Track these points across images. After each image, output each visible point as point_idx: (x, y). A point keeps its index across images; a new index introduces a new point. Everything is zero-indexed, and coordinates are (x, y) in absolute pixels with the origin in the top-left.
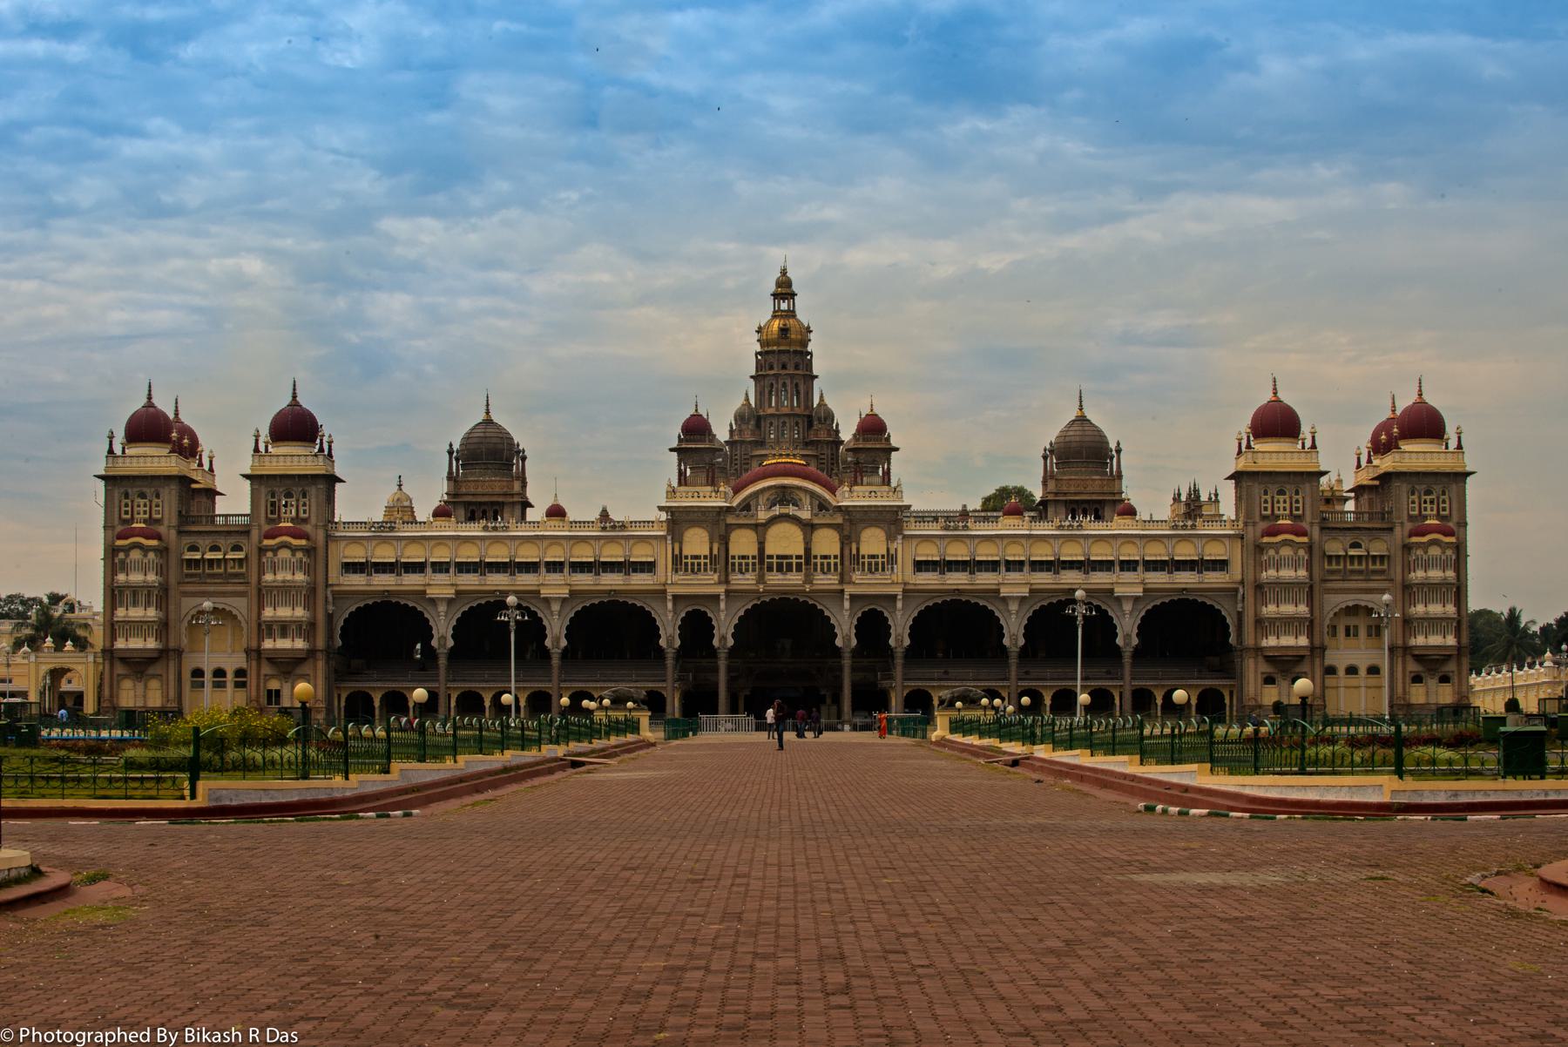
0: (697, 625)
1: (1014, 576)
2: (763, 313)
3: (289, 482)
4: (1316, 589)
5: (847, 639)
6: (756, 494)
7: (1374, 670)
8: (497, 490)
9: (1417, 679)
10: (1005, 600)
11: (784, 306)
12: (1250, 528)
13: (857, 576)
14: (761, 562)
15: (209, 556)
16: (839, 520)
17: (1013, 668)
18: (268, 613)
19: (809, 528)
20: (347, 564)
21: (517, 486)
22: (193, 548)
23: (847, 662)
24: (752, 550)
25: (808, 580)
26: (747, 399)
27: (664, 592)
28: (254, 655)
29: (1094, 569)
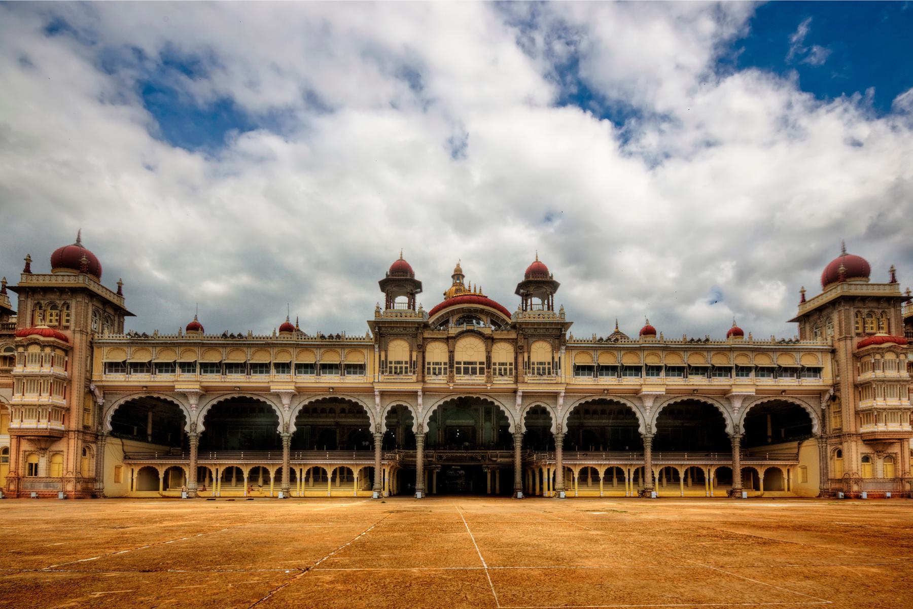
1: (653, 379)
13: (528, 378)
14: (451, 366)
19: (490, 340)
25: (489, 380)
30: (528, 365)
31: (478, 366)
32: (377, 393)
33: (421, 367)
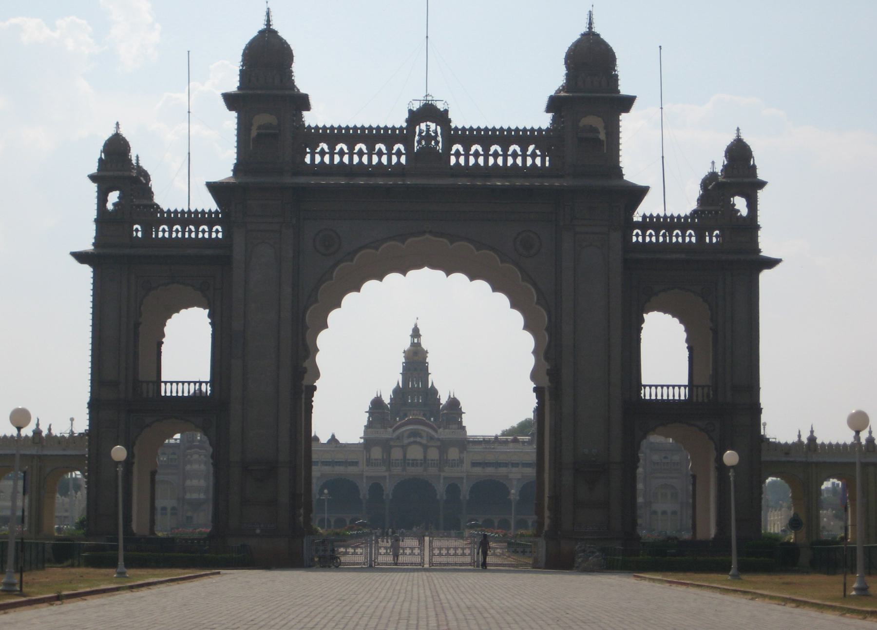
0: (376, 488)
1: (515, 470)
2: (406, 343)
7: (674, 513)
11: (416, 340)
16: (439, 444)
18: (188, 483)
19: (426, 447)
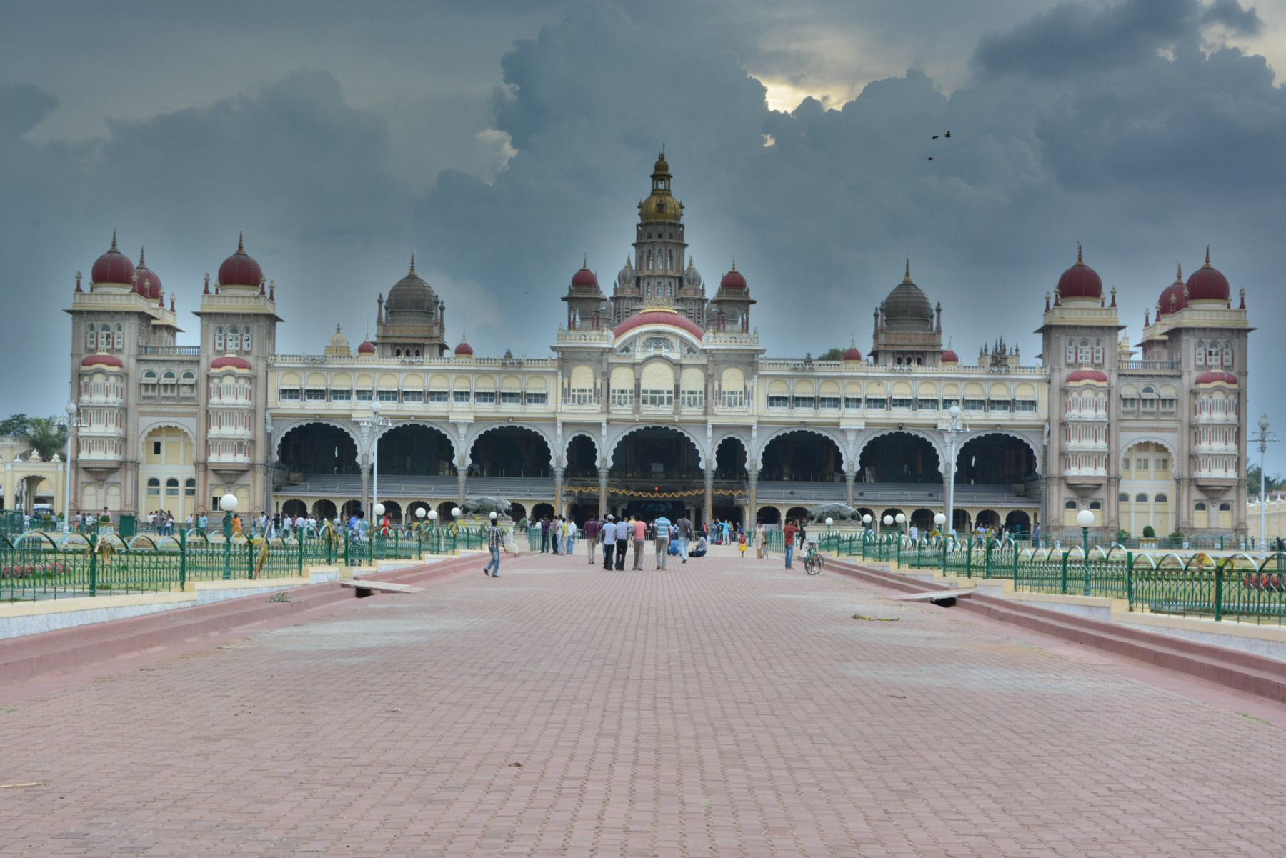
0: (582, 450)
1: (852, 411)
3: (234, 320)
4: (1113, 427)
5: (709, 462)
6: (634, 338)
7: (1161, 498)
8: (419, 334)
9: (1201, 506)
10: (843, 431)
12: (1056, 375)
13: (718, 409)
14: (638, 395)
15: (164, 380)
16: (703, 360)
17: (851, 490)
18: (214, 431)
19: (678, 366)
20: (284, 391)
21: (436, 331)
22: (151, 374)
23: (709, 482)
24: (630, 386)
25: (677, 412)
26: (629, 262)
27: (555, 420)
28: (202, 467)
29: (921, 407)
30: (719, 394)
31: (666, 395)
32: (559, 424)
33: (605, 395)
